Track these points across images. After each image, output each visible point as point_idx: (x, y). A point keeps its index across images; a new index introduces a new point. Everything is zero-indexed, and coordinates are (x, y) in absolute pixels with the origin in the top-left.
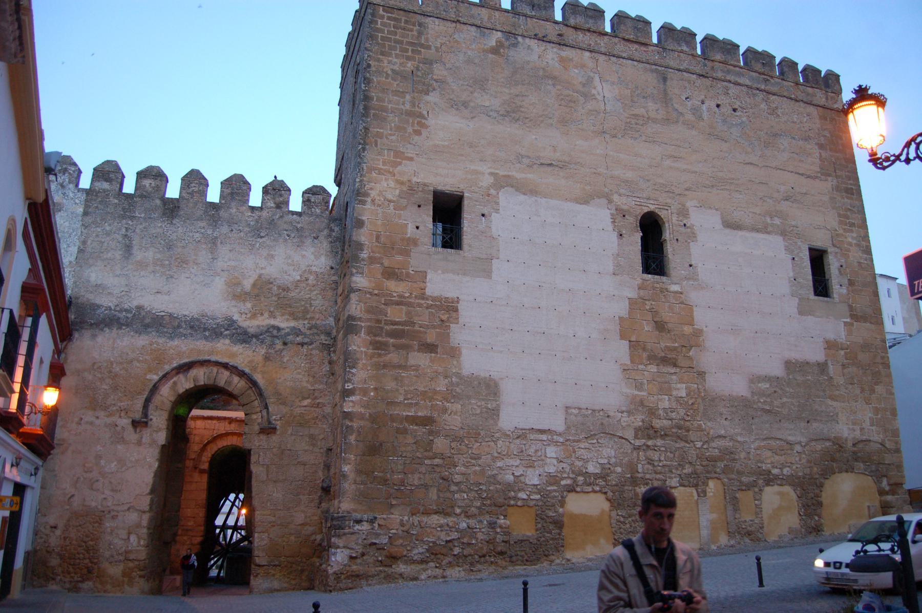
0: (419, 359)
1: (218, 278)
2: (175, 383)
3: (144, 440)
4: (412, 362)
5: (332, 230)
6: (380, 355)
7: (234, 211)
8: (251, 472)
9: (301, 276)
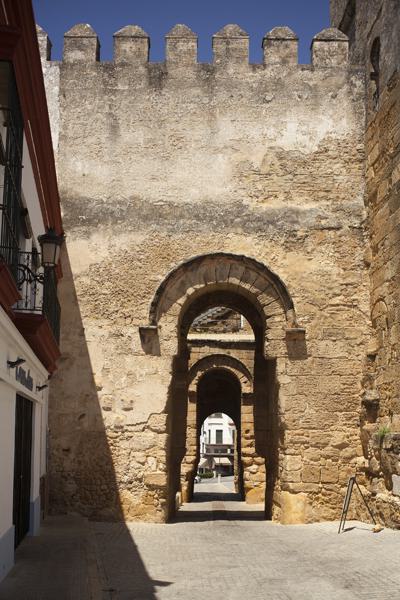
1: (220, 156)
5: (353, 85)
7: (231, 71)
9: (319, 146)
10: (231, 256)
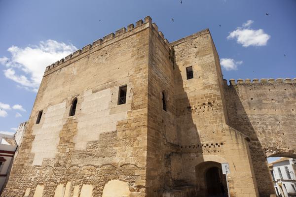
0: (26, 150)
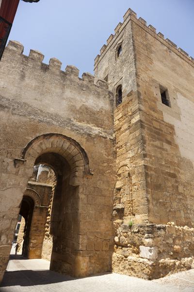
0: (166, 146)
1: (64, 101)
2: (41, 143)
3: (20, 173)
4: (165, 147)
6: (153, 141)
7: (72, 77)
8: (79, 198)
10: (65, 137)
